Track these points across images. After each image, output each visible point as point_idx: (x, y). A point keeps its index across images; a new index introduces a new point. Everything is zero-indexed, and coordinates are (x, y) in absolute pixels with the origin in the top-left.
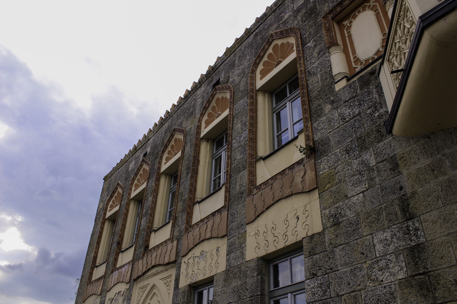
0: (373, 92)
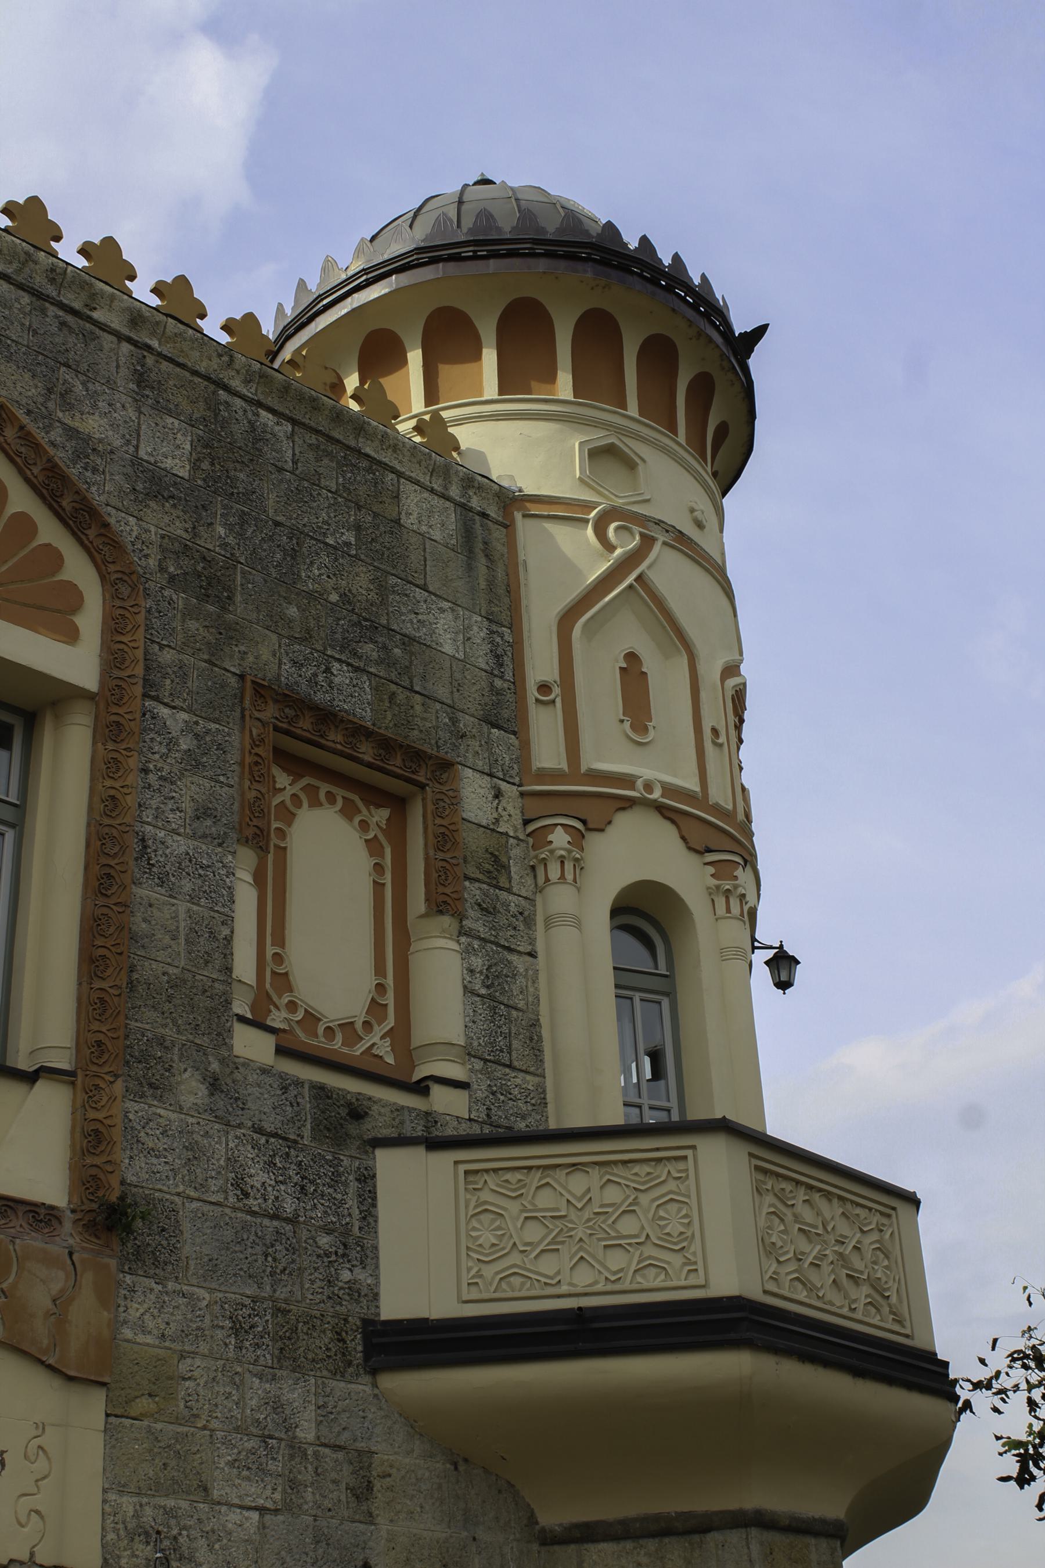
0: (346, 1184)
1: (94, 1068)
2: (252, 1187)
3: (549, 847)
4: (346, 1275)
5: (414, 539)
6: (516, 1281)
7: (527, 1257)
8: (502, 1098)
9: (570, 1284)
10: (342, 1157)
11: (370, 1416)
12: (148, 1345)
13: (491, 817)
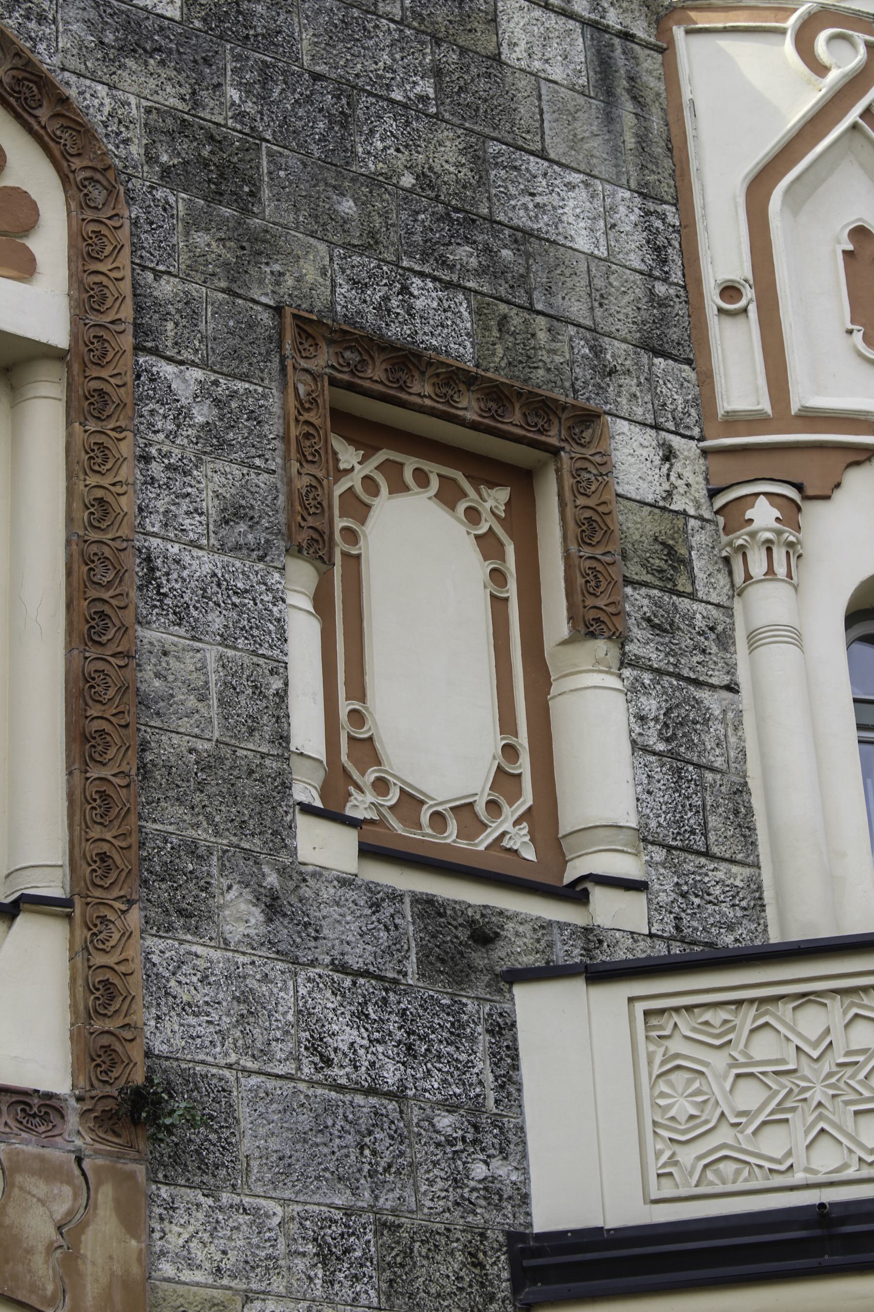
0: (473, 1039)
1: (98, 893)
2: (336, 1050)
3: (748, 529)
4: (479, 1171)
5: (524, 83)
6: (727, 1168)
7: (742, 1132)
8: (697, 901)
9: (807, 1170)
10: (464, 1000)
12: (197, 1284)
13: (659, 490)
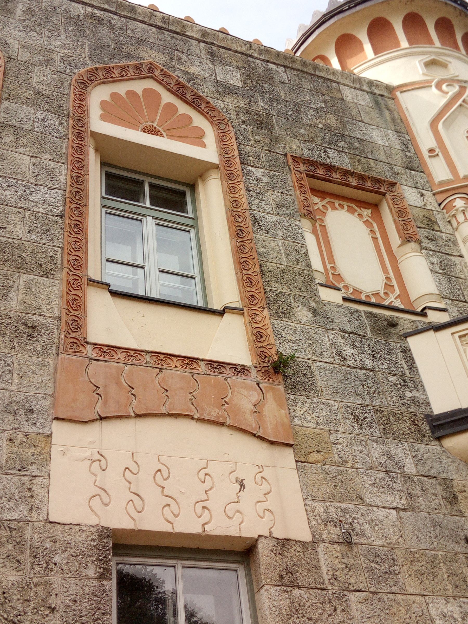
11: (444, 461)
